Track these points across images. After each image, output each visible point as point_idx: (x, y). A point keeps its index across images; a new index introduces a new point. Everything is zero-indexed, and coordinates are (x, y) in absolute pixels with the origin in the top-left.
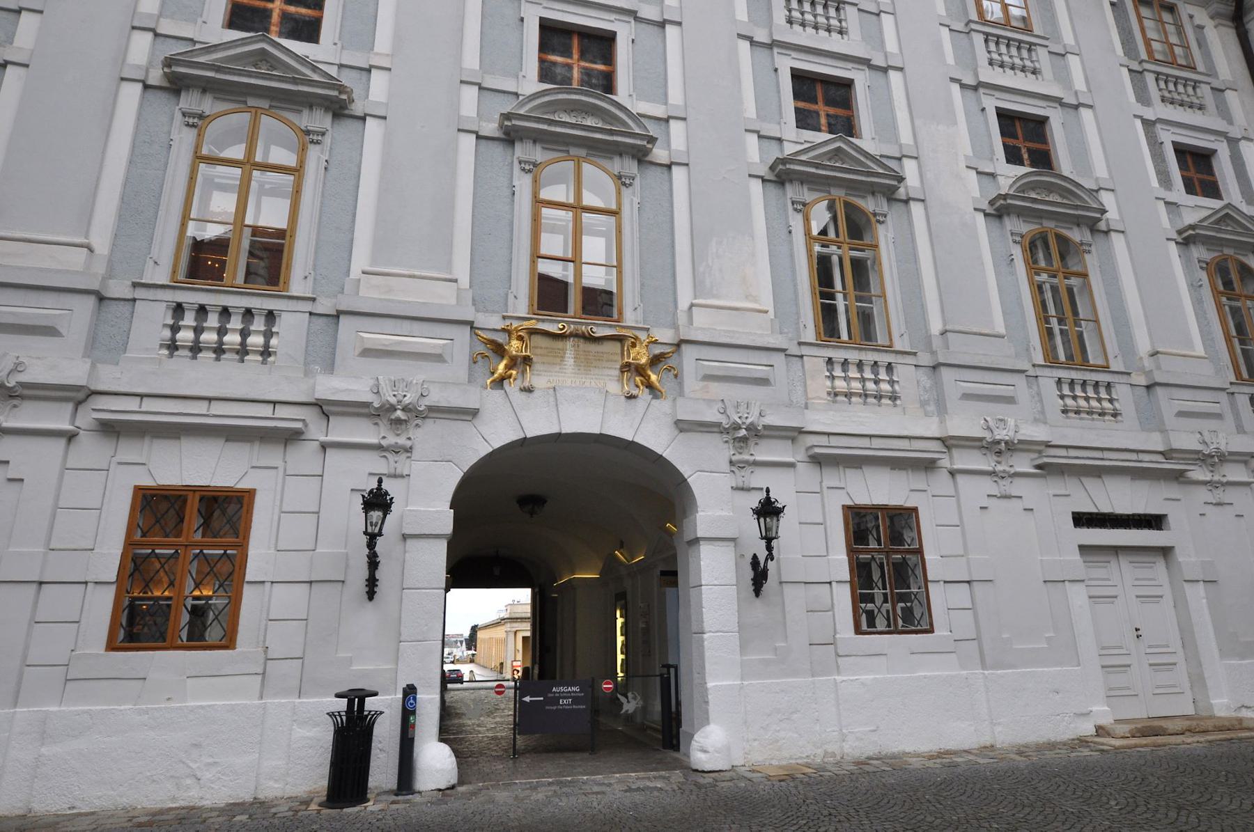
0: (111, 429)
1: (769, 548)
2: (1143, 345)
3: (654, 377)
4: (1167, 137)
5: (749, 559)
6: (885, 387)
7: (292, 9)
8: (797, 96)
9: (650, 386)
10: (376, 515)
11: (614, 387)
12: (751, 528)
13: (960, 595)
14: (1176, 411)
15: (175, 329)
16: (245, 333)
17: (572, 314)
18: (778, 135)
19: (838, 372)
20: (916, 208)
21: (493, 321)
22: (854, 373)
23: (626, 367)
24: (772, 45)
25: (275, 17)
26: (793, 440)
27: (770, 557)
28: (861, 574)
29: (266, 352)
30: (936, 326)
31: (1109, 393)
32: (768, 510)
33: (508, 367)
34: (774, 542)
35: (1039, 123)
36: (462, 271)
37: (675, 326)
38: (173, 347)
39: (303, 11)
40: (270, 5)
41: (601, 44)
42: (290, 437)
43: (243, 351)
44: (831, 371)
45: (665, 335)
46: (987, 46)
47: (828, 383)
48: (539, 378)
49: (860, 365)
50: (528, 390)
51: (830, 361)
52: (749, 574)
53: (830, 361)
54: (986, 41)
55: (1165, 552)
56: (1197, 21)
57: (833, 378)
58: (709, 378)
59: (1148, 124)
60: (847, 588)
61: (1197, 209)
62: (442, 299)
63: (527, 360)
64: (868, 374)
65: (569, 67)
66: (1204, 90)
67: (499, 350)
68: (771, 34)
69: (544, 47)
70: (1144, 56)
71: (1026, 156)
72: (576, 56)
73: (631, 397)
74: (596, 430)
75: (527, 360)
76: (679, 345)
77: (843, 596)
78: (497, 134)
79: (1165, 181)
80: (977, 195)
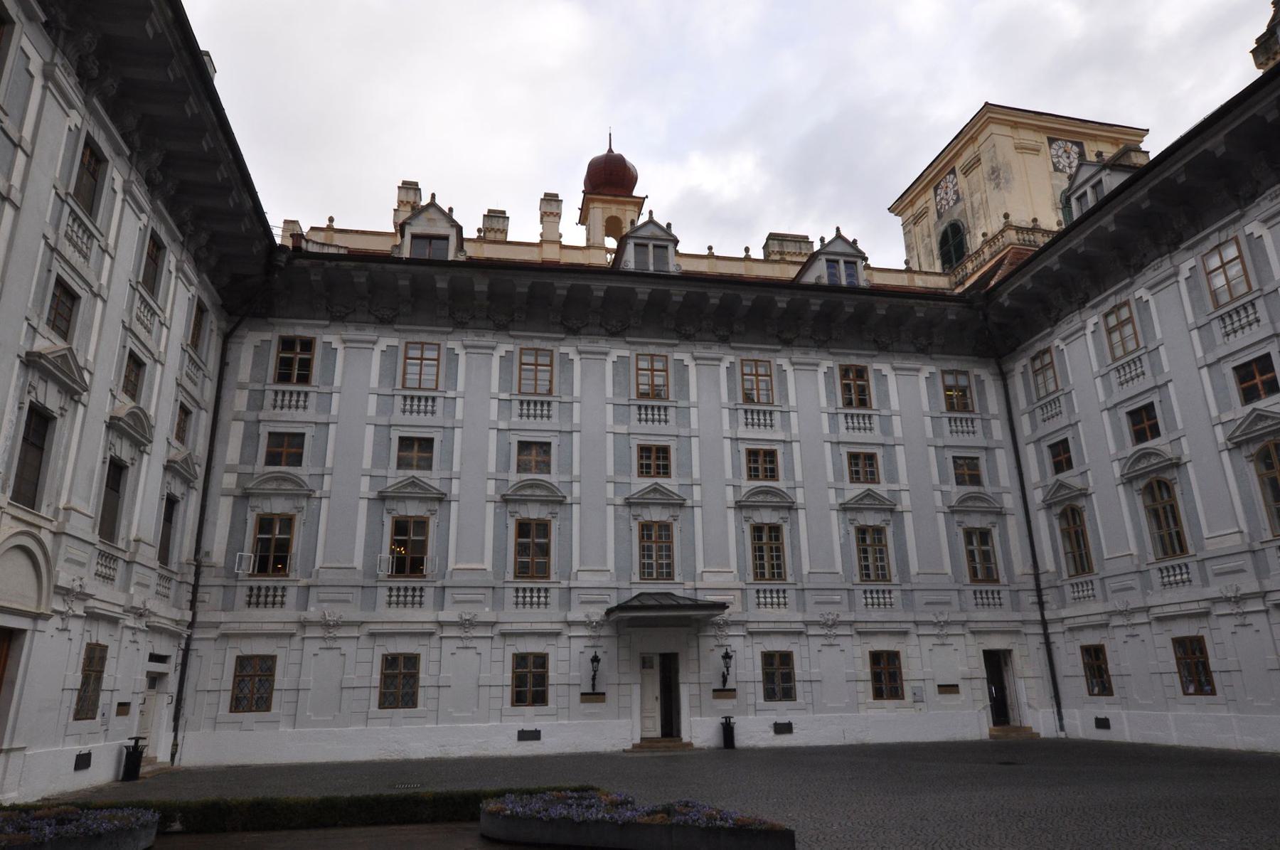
0: (504, 635)
1: (728, 671)
10: (595, 664)
12: (722, 662)
13: (807, 686)
14: (925, 601)
15: (517, 597)
16: (539, 597)
26: (743, 625)
27: (728, 674)
29: (546, 604)
32: (727, 657)
34: (730, 669)
35: (871, 458)
42: (557, 634)
52: (721, 679)
68: (736, 435)
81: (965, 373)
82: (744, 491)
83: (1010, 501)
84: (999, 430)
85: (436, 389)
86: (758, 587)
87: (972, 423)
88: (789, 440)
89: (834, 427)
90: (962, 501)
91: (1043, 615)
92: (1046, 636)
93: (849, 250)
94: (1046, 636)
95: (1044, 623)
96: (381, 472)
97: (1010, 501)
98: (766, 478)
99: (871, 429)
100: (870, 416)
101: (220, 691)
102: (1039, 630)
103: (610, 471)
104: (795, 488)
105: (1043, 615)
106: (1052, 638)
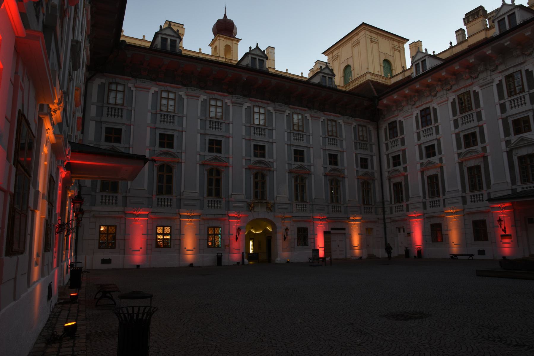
2: (347, 198)
3: (271, 209)
4: (359, 157)
5: (283, 235)
6: (305, 208)
7: (217, 147)
8: (294, 154)
9: (270, 210)
11: (265, 210)
15: (209, 204)
17: (259, 199)
18: (291, 163)
19: (298, 206)
20: (313, 176)
21: (249, 201)
22: (300, 206)
23: (267, 207)
24: (291, 145)
25: (215, 148)
28: (299, 239)
29: (220, 207)
30: (314, 197)
31: (340, 208)
33: (252, 208)
36: (244, 193)
37: (274, 200)
38: (209, 207)
39: (218, 147)
40: (213, 146)
41: (263, 148)
43: (217, 207)
44: (297, 206)
45: (272, 202)
46: (329, 140)
47: (296, 208)
48: (255, 210)
49: (301, 205)
50: (255, 212)
51: (297, 205)
53: (297, 205)
54: (329, 139)
55: (345, 234)
56: (370, 129)
57: (297, 207)
58: (279, 208)
59: (356, 155)
60: (297, 240)
61: (362, 171)
62: (243, 197)
63: (254, 207)
64: (302, 206)
65: (258, 152)
66: (368, 146)
67: (250, 206)
69: (254, 149)
70: (358, 139)
71: (333, 163)
72: (259, 150)
73: (268, 212)
74: (264, 217)
75: (254, 207)
76: (274, 203)
77: (296, 241)
78: (248, 168)
79: (357, 166)
80: (323, 172)
81: (365, 126)
82: (328, 170)
83: (377, 175)
84: (375, 148)
85: (174, 112)
86: (209, 199)
87: (367, 145)
88: (309, 146)
89: (289, 139)
90: (331, 170)
91: (384, 216)
92: (385, 223)
93: (330, 73)
94: (385, 223)
95: (384, 219)
96: (249, 158)
97: (377, 175)
98: (300, 161)
99: (303, 140)
100: (336, 140)
101: (294, 239)
102: (382, 221)
103: (244, 155)
104: (311, 166)
105: (384, 216)
106: (387, 224)
